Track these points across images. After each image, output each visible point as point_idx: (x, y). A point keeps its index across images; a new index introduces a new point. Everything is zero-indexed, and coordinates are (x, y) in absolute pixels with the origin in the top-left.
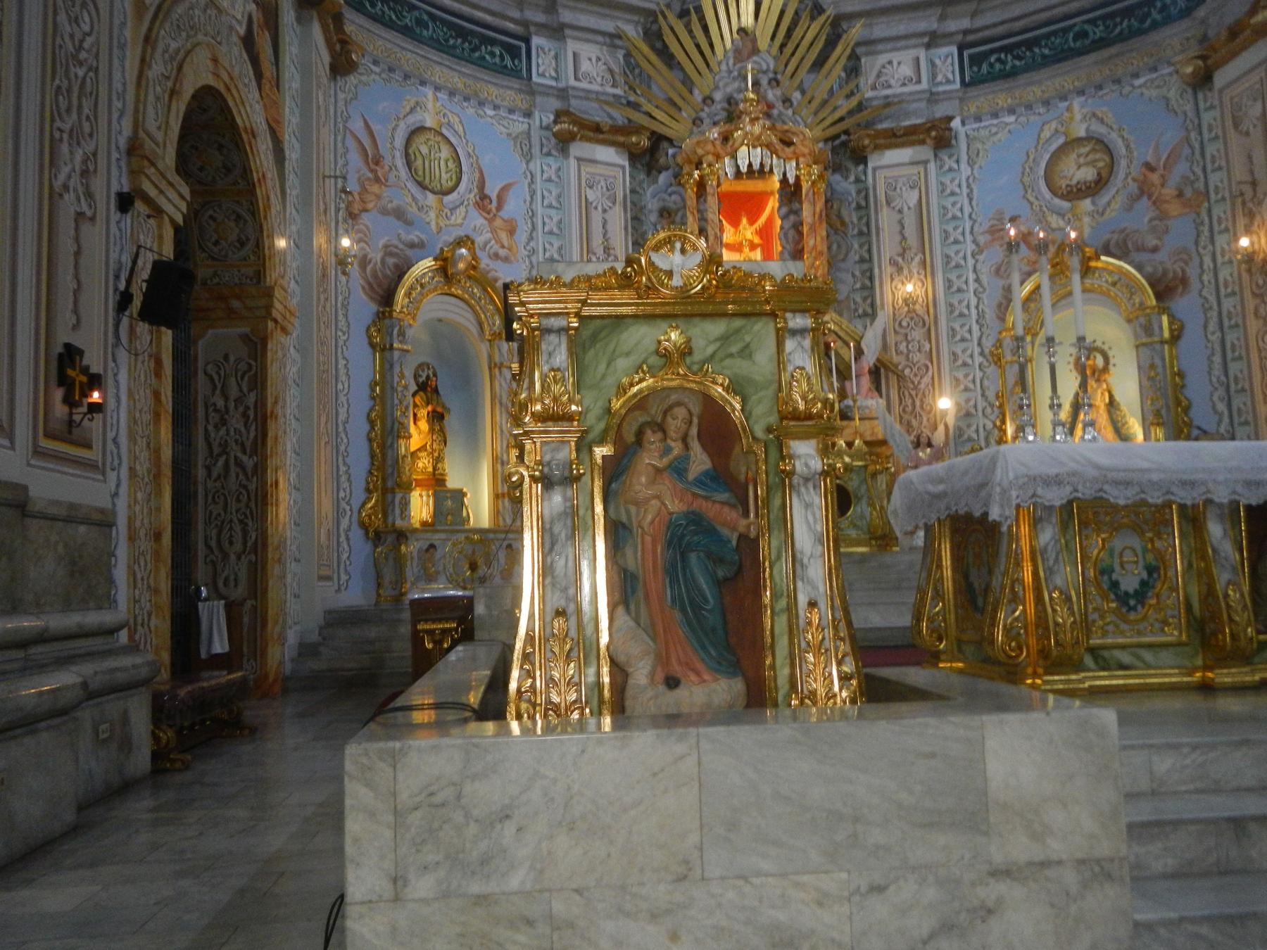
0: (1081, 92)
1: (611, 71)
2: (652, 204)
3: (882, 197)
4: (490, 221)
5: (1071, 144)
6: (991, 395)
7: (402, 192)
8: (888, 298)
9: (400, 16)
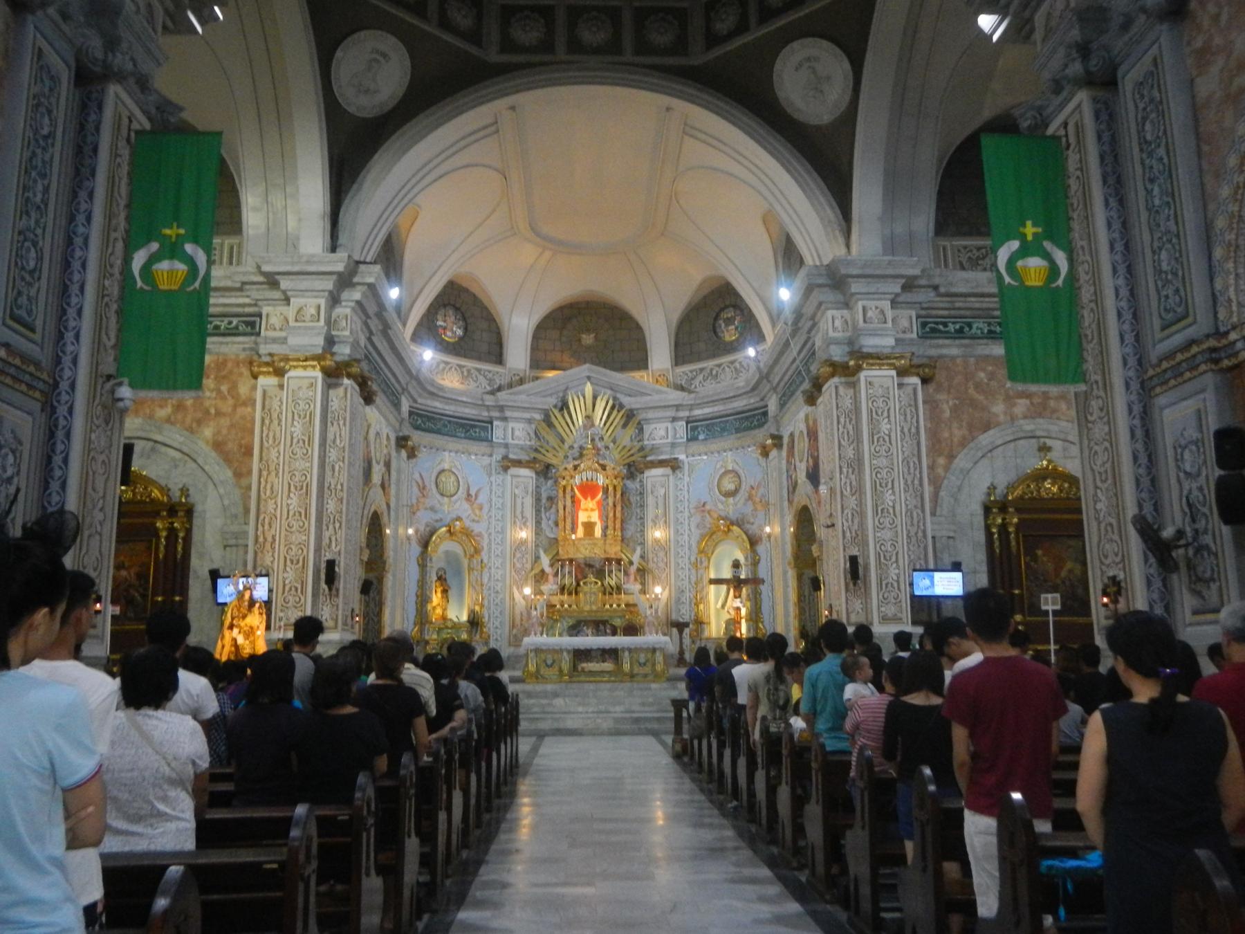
0: (731, 450)
1: (529, 434)
2: (544, 496)
3: (649, 491)
4: (472, 505)
5: (727, 472)
6: (693, 582)
7: (434, 498)
8: (650, 537)
9: (435, 425)
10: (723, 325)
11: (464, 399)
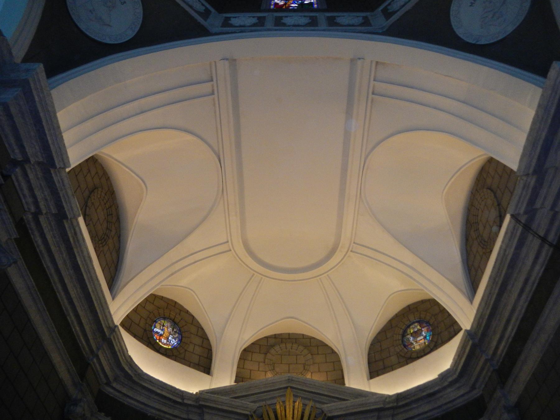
10: (411, 339)
11: (164, 393)
